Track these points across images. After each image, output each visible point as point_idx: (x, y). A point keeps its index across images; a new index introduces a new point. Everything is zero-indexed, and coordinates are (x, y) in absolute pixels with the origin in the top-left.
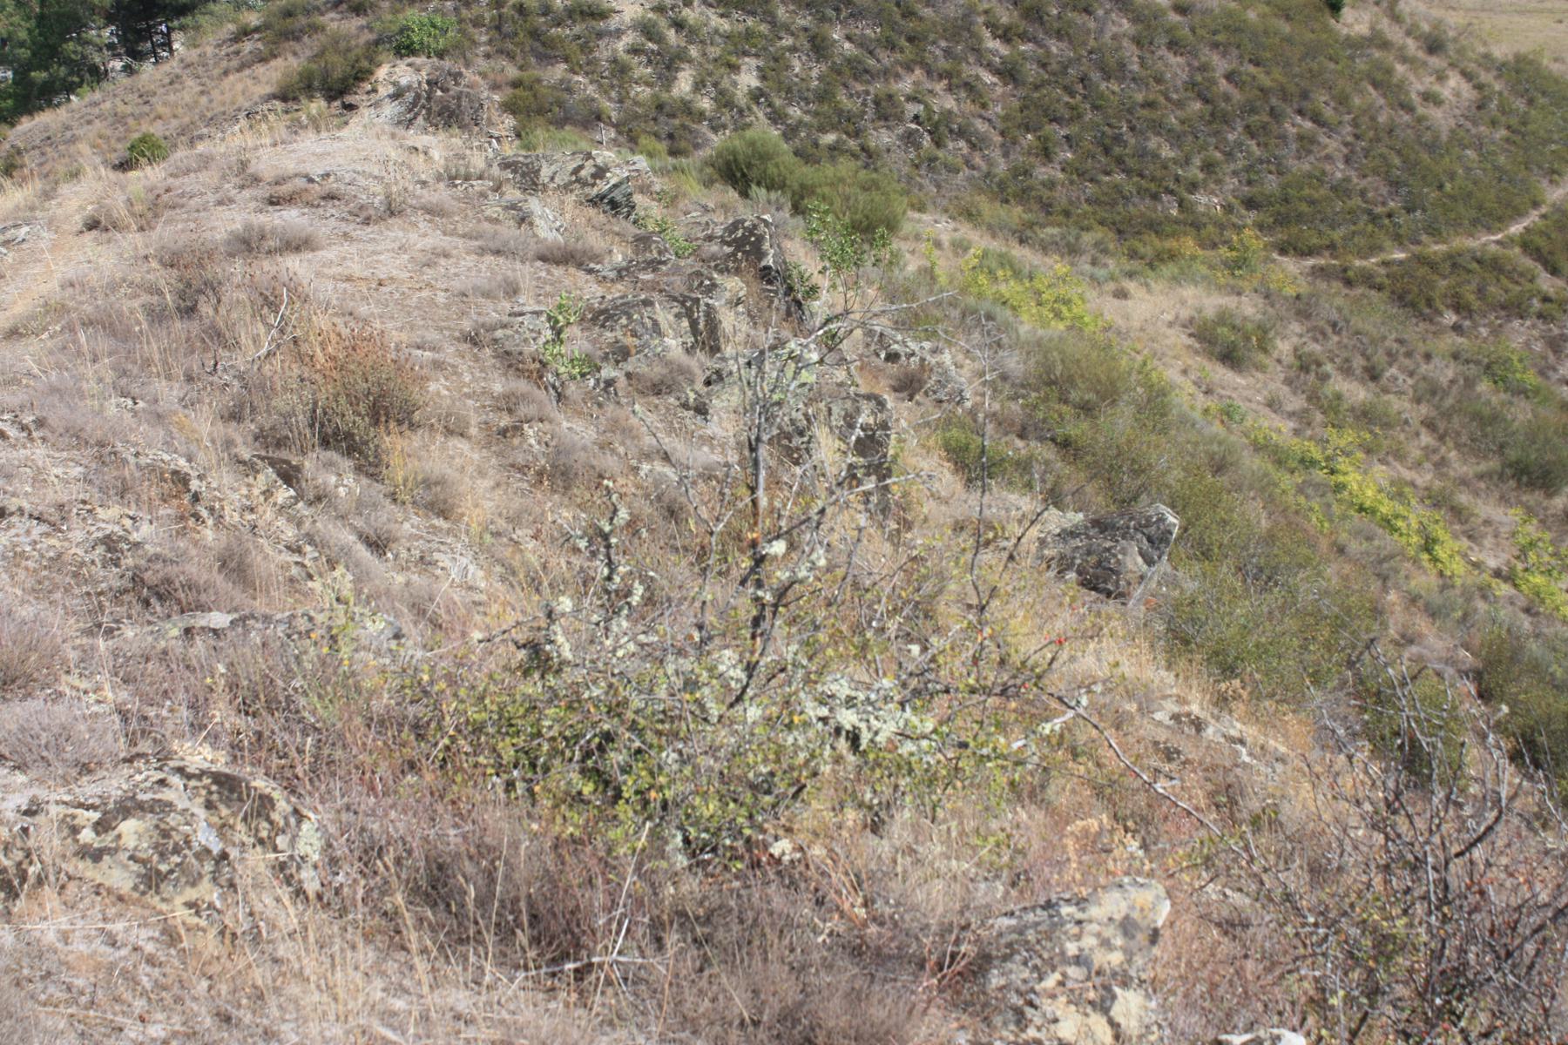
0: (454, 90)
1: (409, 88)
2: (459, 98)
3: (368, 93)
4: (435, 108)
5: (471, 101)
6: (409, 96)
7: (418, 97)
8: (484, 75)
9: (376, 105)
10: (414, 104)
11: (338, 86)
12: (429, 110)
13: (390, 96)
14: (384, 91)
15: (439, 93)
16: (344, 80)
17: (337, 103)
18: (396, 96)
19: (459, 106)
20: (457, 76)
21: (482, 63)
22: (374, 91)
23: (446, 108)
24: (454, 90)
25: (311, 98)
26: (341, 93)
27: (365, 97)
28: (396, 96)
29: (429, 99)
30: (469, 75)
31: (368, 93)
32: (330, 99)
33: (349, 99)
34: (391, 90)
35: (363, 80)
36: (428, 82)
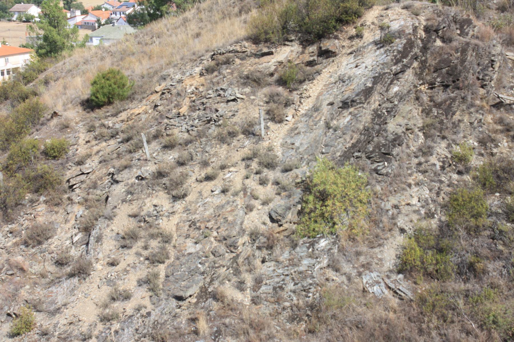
0: (458, 41)
1: (400, 33)
2: (464, 51)
3: (351, 38)
4: (432, 62)
5: (479, 56)
6: (399, 44)
7: (410, 44)
8: (498, 29)
9: (356, 53)
10: (404, 53)
11: (317, 28)
12: (423, 63)
13: (376, 43)
14: (370, 36)
15: (439, 43)
16: (324, 21)
17: (313, 48)
18: (380, 44)
19: (463, 61)
20: (463, 24)
21: (493, 14)
22: (359, 36)
23: (447, 62)
24: (458, 41)
25: (285, 41)
26: (320, 37)
27: (346, 43)
28: (380, 44)
29: (425, 49)
30: (479, 26)
31: (351, 38)
32: (305, 43)
33: (327, 44)
34: (378, 35)
35: (347, 23)
36: (427, 29)
